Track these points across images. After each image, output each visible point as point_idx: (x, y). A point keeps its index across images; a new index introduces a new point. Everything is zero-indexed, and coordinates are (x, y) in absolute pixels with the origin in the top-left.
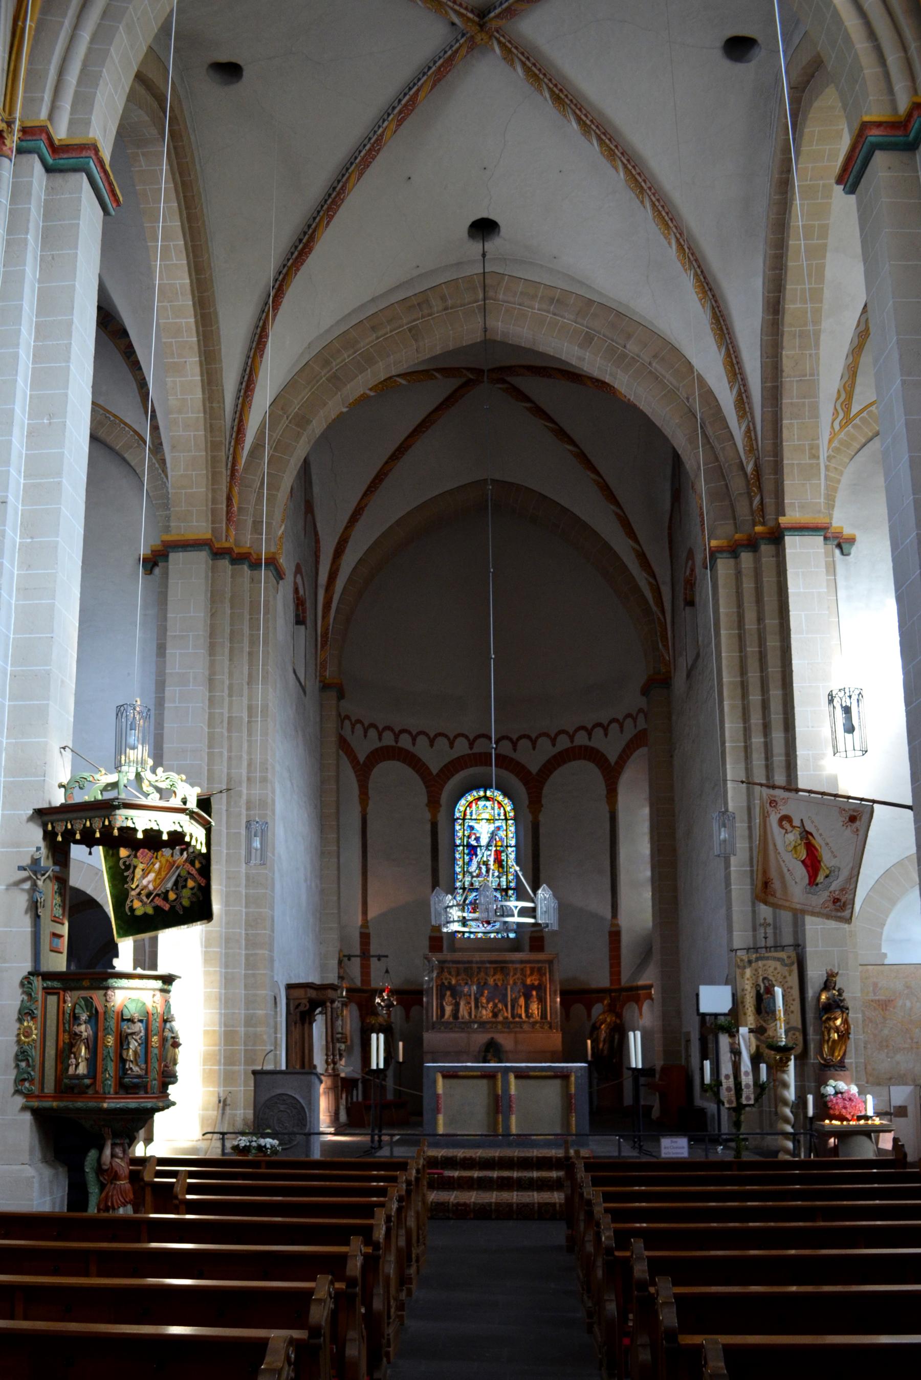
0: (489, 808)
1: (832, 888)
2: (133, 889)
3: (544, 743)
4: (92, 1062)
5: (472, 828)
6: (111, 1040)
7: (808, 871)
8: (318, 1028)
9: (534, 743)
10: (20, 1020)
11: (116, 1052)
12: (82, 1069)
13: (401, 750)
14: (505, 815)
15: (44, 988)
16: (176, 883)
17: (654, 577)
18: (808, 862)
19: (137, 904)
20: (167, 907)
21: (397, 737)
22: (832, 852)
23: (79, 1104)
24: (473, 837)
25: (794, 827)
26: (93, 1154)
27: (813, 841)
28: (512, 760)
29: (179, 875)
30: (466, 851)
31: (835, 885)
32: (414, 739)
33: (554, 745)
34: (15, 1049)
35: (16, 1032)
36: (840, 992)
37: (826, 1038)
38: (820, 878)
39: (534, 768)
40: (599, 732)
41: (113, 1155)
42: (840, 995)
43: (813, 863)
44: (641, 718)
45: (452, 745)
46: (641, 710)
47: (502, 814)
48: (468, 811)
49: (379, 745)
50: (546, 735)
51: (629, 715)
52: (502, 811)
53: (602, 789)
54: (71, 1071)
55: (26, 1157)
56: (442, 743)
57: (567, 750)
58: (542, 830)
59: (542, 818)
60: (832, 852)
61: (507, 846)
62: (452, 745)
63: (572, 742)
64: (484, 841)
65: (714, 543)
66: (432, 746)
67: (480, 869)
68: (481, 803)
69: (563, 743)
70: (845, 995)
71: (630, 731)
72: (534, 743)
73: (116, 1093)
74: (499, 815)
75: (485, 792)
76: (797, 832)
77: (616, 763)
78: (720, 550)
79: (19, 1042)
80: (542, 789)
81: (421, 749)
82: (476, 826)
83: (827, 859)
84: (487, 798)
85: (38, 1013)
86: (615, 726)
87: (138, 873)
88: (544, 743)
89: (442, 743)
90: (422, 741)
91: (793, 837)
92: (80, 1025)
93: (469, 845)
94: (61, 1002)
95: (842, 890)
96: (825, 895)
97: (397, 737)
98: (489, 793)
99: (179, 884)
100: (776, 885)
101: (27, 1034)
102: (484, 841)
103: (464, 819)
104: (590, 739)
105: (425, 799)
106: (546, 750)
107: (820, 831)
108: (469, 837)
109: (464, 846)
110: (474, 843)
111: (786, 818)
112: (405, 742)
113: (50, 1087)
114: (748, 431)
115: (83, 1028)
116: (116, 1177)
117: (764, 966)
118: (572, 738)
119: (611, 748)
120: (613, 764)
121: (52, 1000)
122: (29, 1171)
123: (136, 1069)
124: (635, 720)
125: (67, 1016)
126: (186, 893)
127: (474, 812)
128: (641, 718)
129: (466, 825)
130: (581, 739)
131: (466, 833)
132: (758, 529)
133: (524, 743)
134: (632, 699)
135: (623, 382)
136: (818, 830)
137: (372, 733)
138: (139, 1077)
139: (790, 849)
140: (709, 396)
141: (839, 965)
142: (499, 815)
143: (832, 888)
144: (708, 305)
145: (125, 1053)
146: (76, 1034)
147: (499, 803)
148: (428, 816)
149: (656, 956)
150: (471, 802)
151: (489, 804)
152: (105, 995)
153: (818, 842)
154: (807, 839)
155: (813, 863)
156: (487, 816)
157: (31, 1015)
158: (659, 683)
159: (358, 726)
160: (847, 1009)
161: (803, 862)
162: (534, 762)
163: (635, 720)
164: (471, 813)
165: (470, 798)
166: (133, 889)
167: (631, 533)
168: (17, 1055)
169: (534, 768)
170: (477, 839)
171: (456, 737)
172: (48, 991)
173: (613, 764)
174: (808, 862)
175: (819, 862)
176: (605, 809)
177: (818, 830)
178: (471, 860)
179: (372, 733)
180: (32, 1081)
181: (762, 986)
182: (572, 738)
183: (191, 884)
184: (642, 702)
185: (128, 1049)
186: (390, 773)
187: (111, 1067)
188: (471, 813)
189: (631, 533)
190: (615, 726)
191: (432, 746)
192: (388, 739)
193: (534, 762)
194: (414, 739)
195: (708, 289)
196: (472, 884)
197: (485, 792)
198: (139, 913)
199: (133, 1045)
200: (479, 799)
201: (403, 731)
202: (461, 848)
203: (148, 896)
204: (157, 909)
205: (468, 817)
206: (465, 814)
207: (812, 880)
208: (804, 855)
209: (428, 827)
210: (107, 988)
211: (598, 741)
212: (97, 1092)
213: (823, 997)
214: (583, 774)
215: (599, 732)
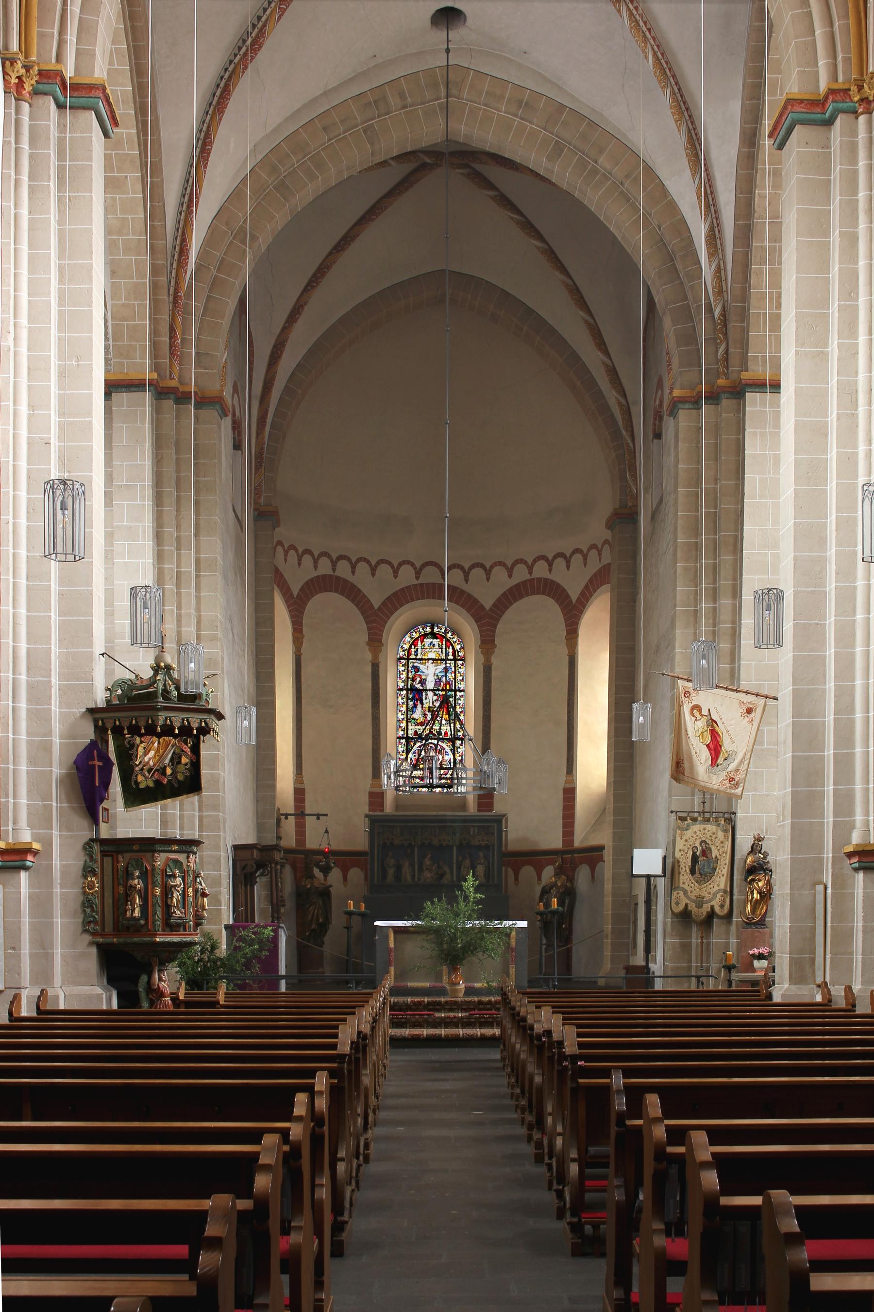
0: (437, 646)
1: (729, 769)
2: (137, 766)
3: (499, 573)
4: (144, 908)
5: (417, 669)
6: (158, 891)
7: (711, 754)
8: (259, 891)
9: (488, 572)
10: (85, 877)
11: (162, 901)
12: (137, 913)
13: (338, 579)
14: (454, 655)
15: (101, 851)
16: (172, 760)
17: (625, 396)
18: (712, 746)
19: (140, 778)
20: (165, 781)
21: (334, 564)
22: (731, 738)
23: (136, 939)
24: (418, 679)
25: (702, 716)
26: (144, 978)
27: (717, 729)
28: (463, 592)
29: (174, 753)
30: (410, 696)
31: (732, 767)
32: (353, 567)
33: (510, 576)
34: (81, 898)
35: (81, 886)
36: (766, 855)
37: (750, 898)
38: (720, 760)
39: (488, 603)
40: (560, 563)
41: (160, 979)
42: (765, 858)
43: (715, 748)
44: (606, 550)
45: (396, 573)
46: (606, 542)
47: (451, 654)
48: (413, 650)
49: (314, 574)
50: (502, 564)
51: (593, 546)
52: (451, 650)
53: (562, 631)
54: (128, 914)
55: (95, 981)
56: (385, 571)
57: (524, 582)
58: (494, 674)
59: (494, 660)
60: (731, 738)
61: (455, 691)
62: (396, 573)
63: (530, 573)
64: (430, 685)
65: (677, 393)
66: (373, 575)
67: (425, 715)
68: (427, 641)
69: (521, 574)
70: (769, 858)
71: (594, 565)
72: (488, 572)
73: (163, 931)
74: (447, 654)
75: (432, 628)
76: (704, 719)
77: (578, 600)
78: (682, 400)
79: (84, 893)
80: (495, 626)
81: (362, 579)
82: (422, 667)
83: (727, 745)
84: (434, 636)
85: (98, 870)
86: (578, 557)
87: (141, 750)
88: (499, 573)
89: (385, 571)
90: (362, 567)
91: (701, 724)
92: (134, 879)
93: (413, 689)
94: (115, 862)
95: (737, 770)
96: (723, 775)
97: (334, 564)
98: (436, 630)
99: (176, 760)
100: (686, 765)
101: (91, 887)
102: (430, 685)
103: (408, 659)
104: (550, 570)
105: (365, 637)
106: (502, 582)
107: (723, 720)
108: (413, 680)
109: (407, 690)
110: (419, 686)
111: (697, 707)
112: (343, 570)
113: (109, 928)
114: (718, 270)
115: (136, 881)
116: (162, 994)
117: (704, 829)
118: (530, 568)
119: (573, 582)
120: (574, 600)
121: (108, 860)
122: (98, 990)
123: (178, 912)
124: (600, 553)
125: (120, 873)
126: (181, 768)
127: (419, 651)
128: (606, 550)
129: (411, 665)
130: (541, 571)
131: (410, 675)
132: (721, 382)
133: (478, 573)
134: (597, 530)
135: (593, 198)
136: (721, 719)
137: (307, 560)
138: (181, 918)
139: (698, 734)
140: (682, 227)
141: (767, 830)
142: (447, 654)
143: (729, 769)
144: (684, 128)
145: (169, 900)
146: (131, 886)
147: (448, 641)
148: (369, 656)
149: (610, 818)
150: (417, 639)
151: (436, 642)
152: (153, 856)
153: (721, 729)
154: (712, 726)
155: (715, 748)
156: (432, 655)
157: (93, 872)
158: (625, 517)
159: (292, 553)
160: (771, 871)
161: (708, 746)
162: (487, 594)
163: (600, 553)
164: (416, 652)
165: (415, 635)
166: (137, 766)
167: (601, 344)
168: (83, 903)
169: (488, 603)
170: (423, 682)
171: (400, 565)
172: (104, 854)
173: (574, 600)
174: (712, 746)
175: (720, 746)
176: (564, 651)
177: (721, 719)
178: (415, 706)
179: (307, 560)
180: (95, 922)
181: (700, 848)
182: (530, 568)
183: (184, 760)
184: (608, 535)
185: (172, 896)
186: (326, 606)
187: (159, 911)
188: (416, 652)
189: (601, 344)
190: (578, 557)
191: (373, 575)
192: (325, 567)
193: (487, 594)
194: (353, 567)
195: (684, 109)
196: (416, 732)
197: (432, 628)
198: (142, 786)
199: (176, 895)
200: (425, 636)
201: (341, 557)
202: (405, 692)
203: (149, 771)
204: (158, 783)
205: (413, 656)
206: (409, 654)
207: (714, 762)
208: (708, 740)
209: (369, 669)
210: (154, 851)
211: (560, 574)
212: (149, 930)
213: (750, 859)
214: (543, 611)
215: (560, 563)
